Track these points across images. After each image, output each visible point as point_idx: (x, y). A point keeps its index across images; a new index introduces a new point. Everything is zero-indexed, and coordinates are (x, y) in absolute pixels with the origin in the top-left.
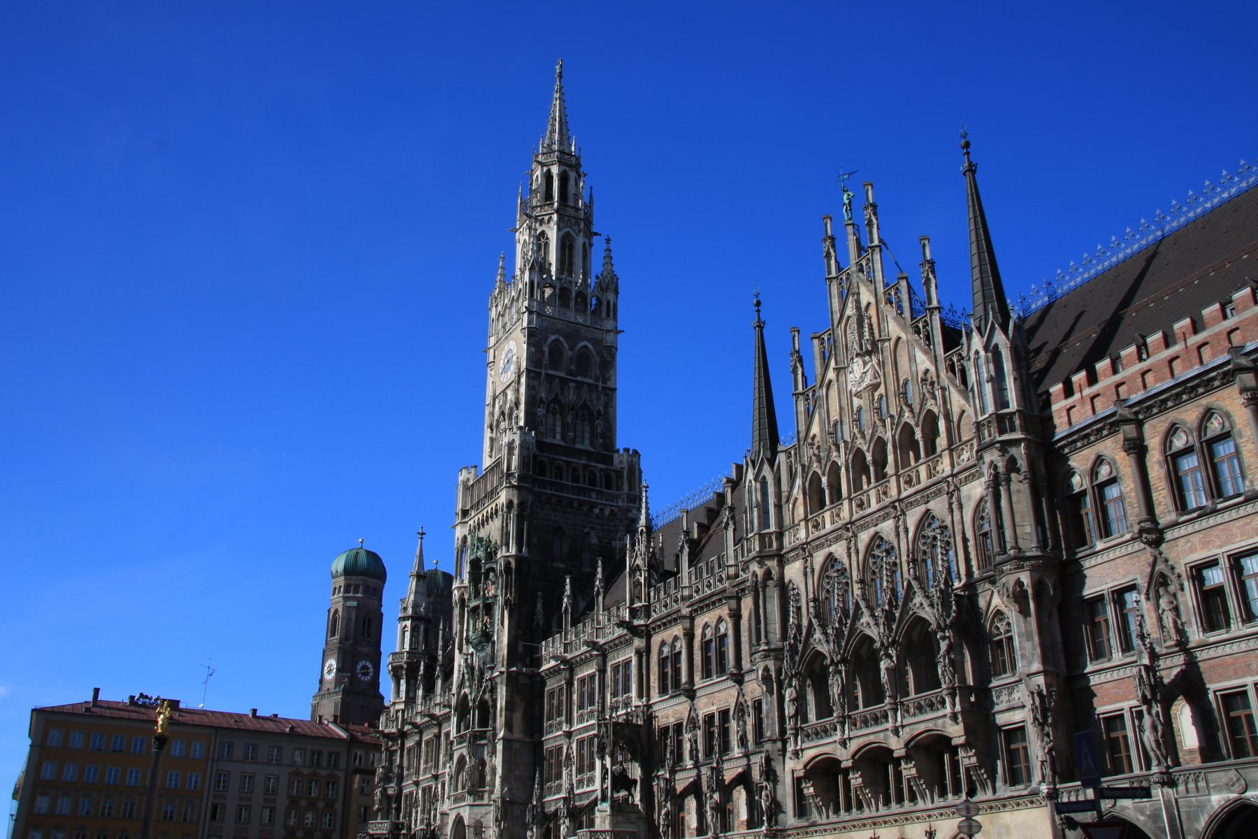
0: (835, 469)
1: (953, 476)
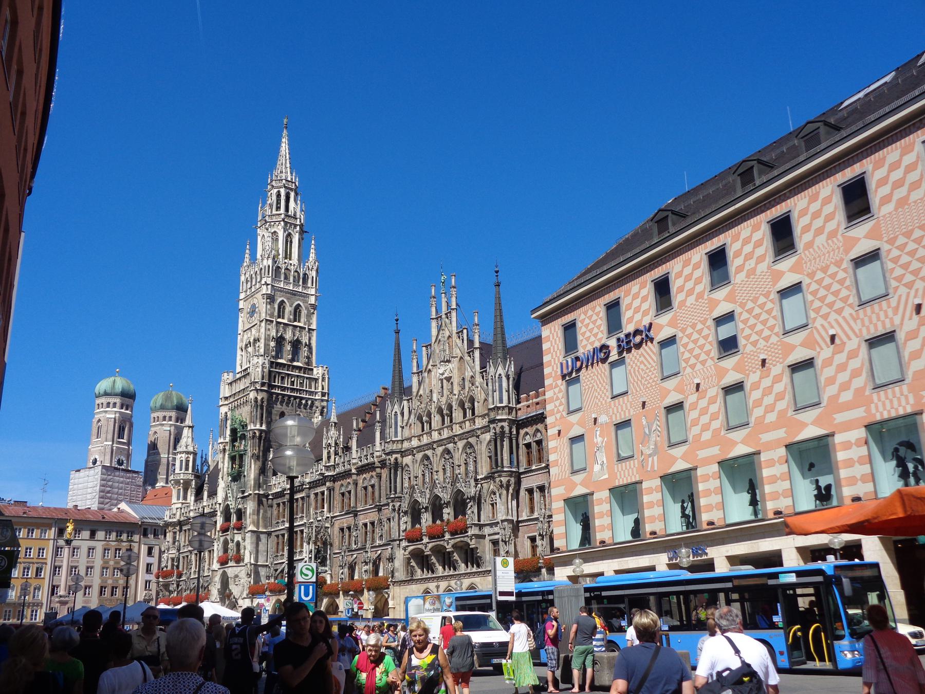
0: (429, 415)
1: (478, 429)
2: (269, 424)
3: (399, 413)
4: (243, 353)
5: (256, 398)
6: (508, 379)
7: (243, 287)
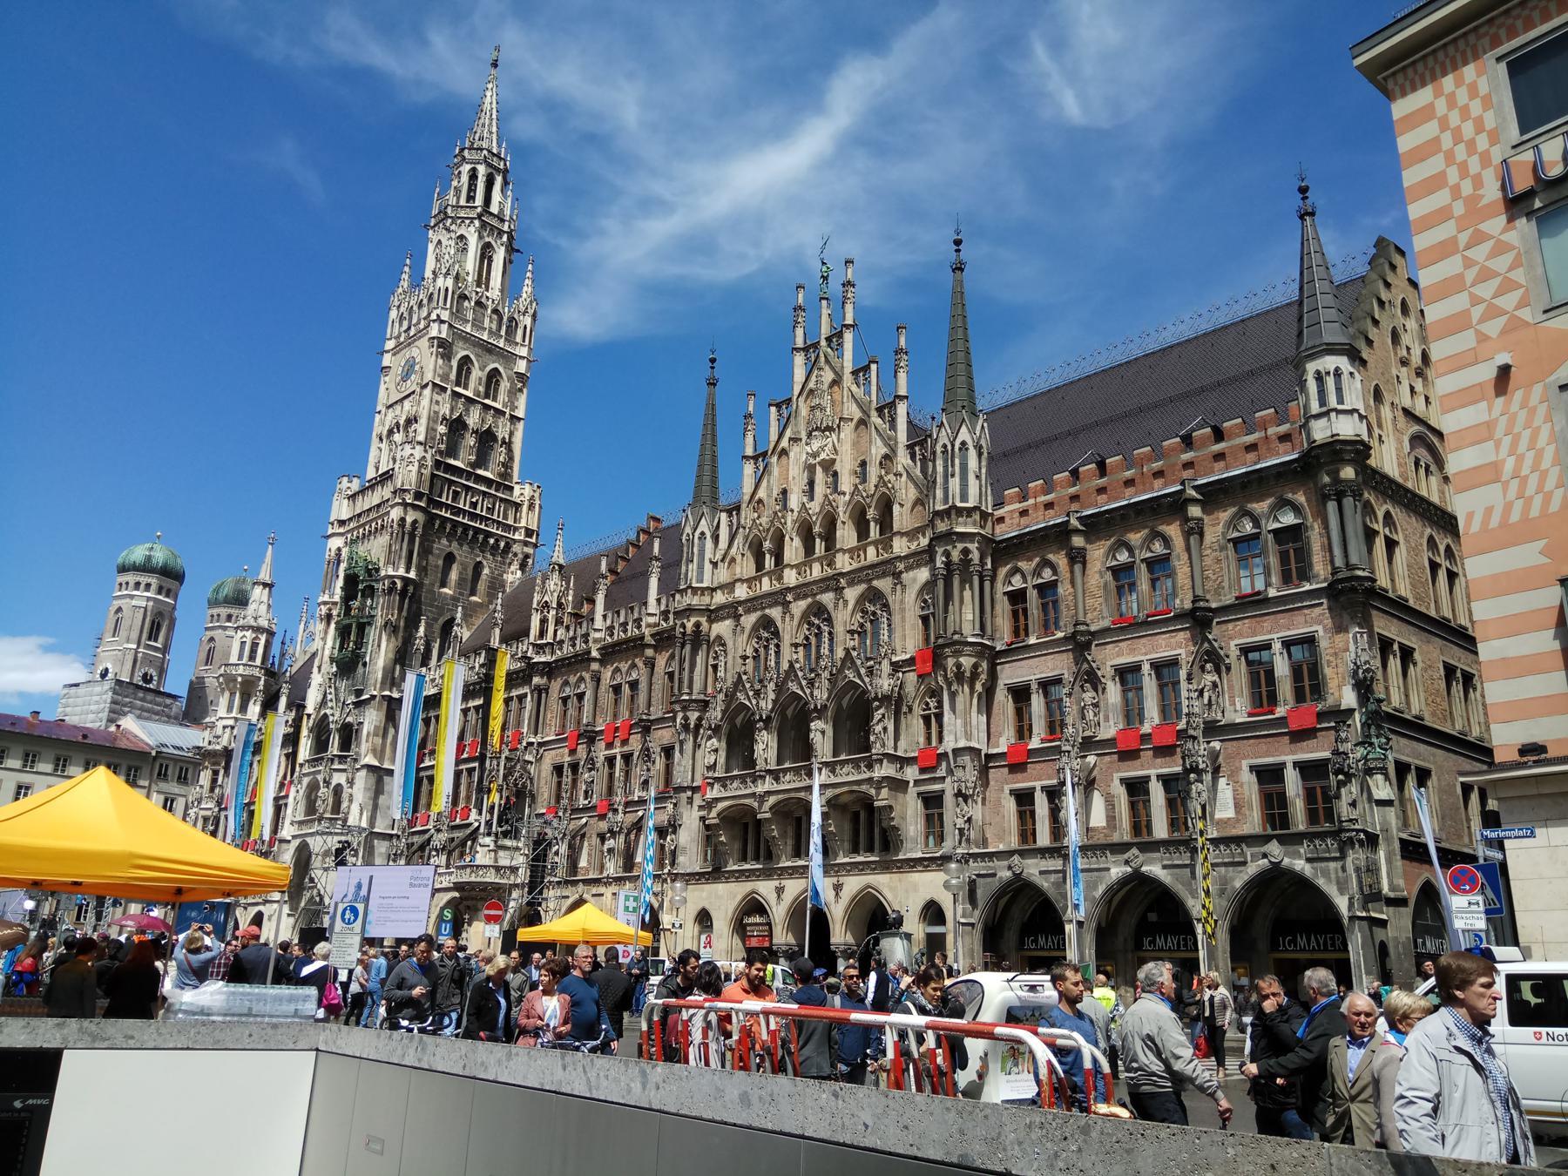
2: (422, 570)
3: (708, 535)
4: (384, 446)
5: (403, 520)
6: (980, 455)
7: (394, 329)
